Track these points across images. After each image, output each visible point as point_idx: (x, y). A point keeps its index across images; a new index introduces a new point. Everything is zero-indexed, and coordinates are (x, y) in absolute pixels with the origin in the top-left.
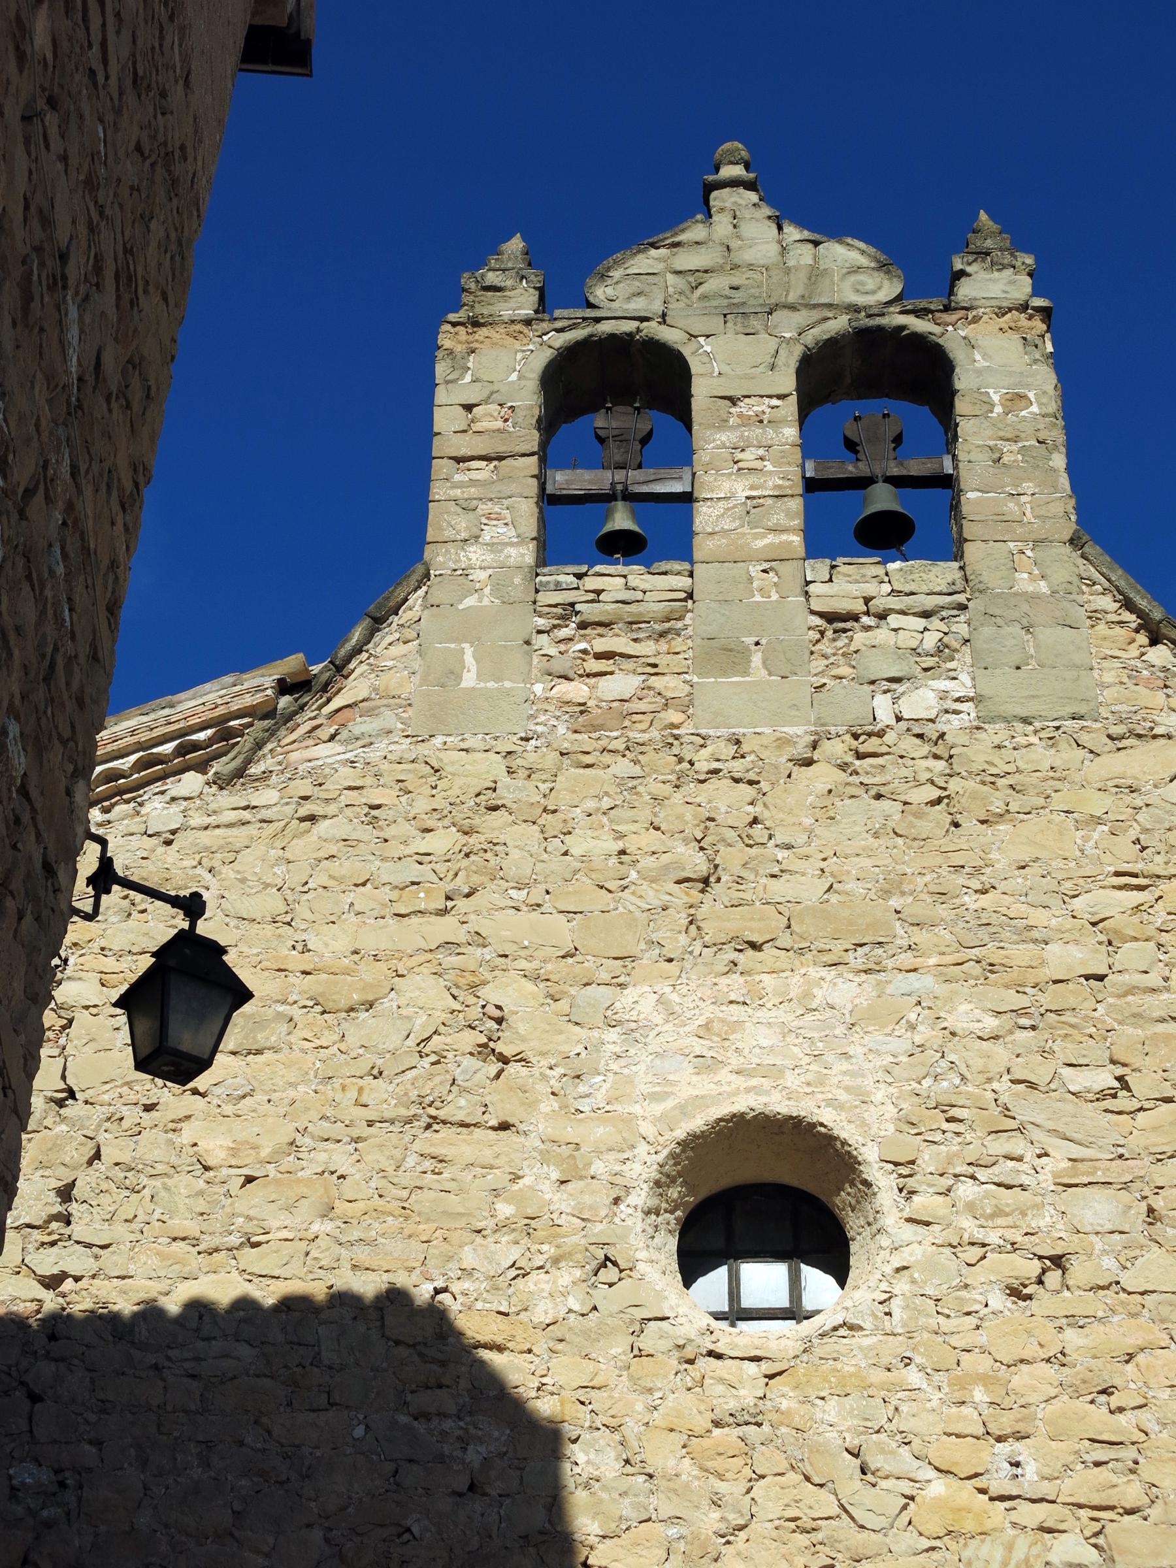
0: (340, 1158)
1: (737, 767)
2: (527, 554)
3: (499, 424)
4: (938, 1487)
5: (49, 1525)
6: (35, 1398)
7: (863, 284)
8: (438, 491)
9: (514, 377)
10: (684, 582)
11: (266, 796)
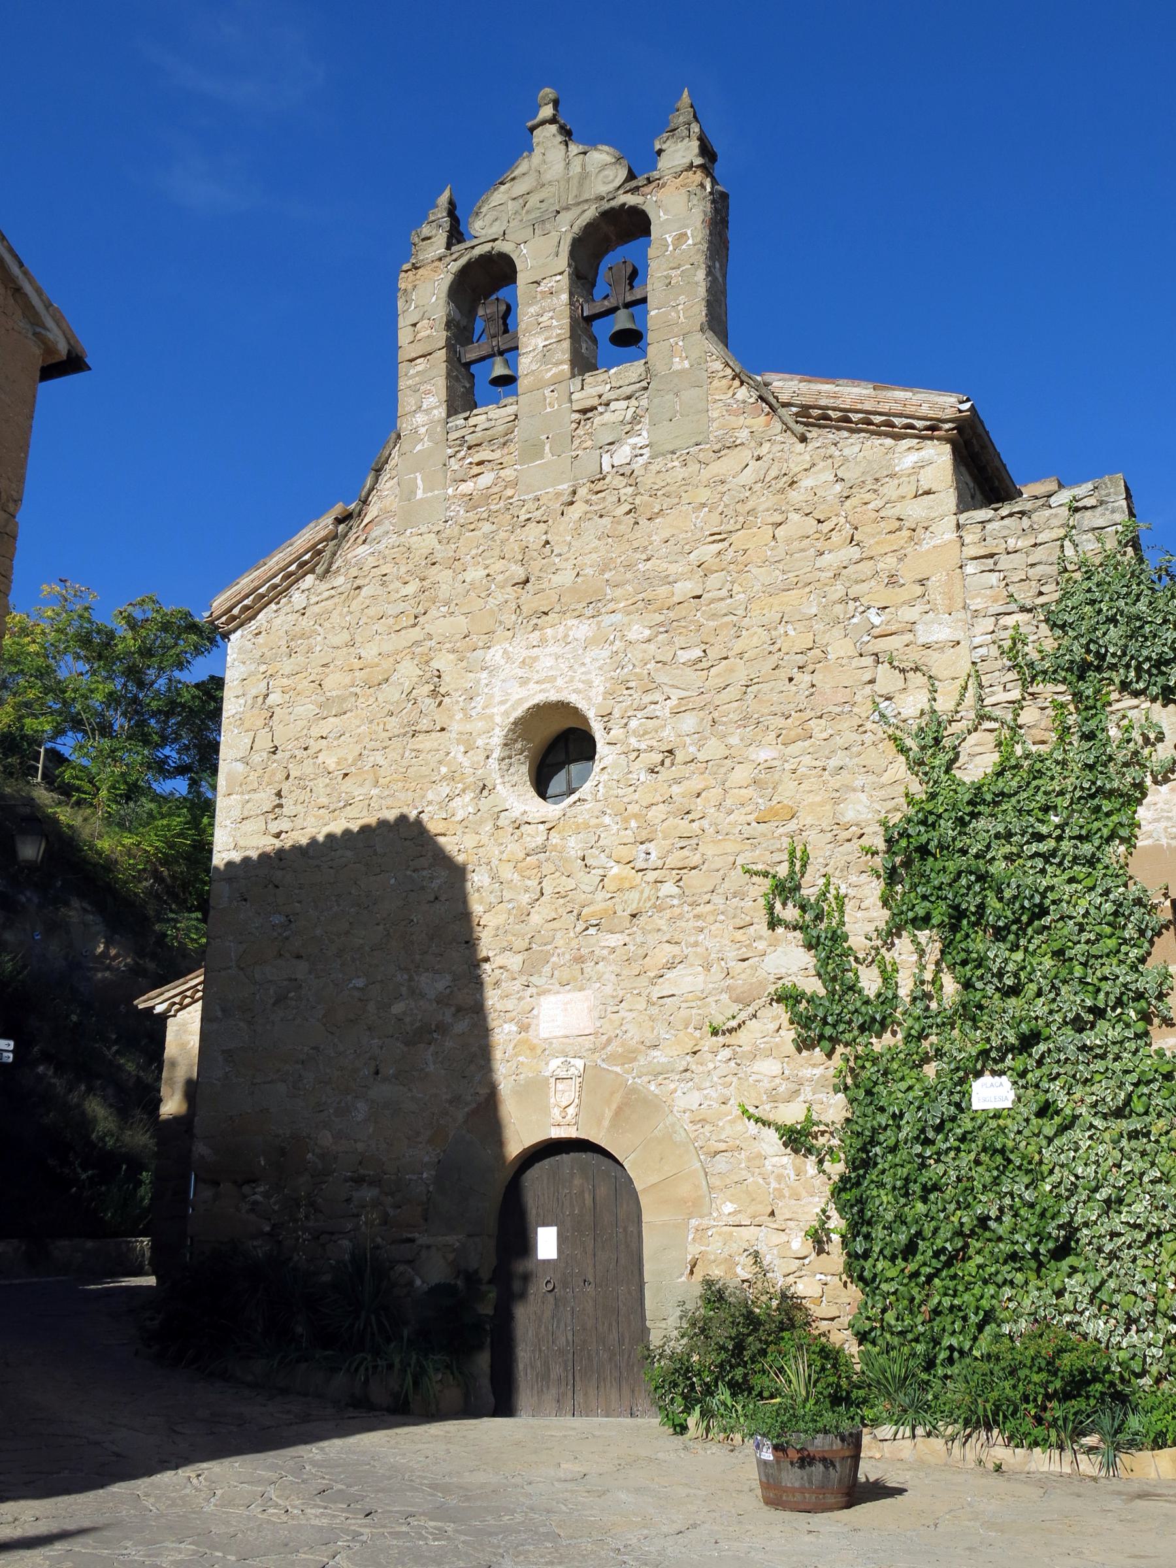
0: (378, 757)
1: (537, 515)
2: (441, 412)
3: (429, 332)
4: (616, 870)
5: (287, 938)
6: (277, 887)
7: (606, 177)
8: (403, 383)
9: (434, 299)
10: (511, 409)
11: (339, 580)
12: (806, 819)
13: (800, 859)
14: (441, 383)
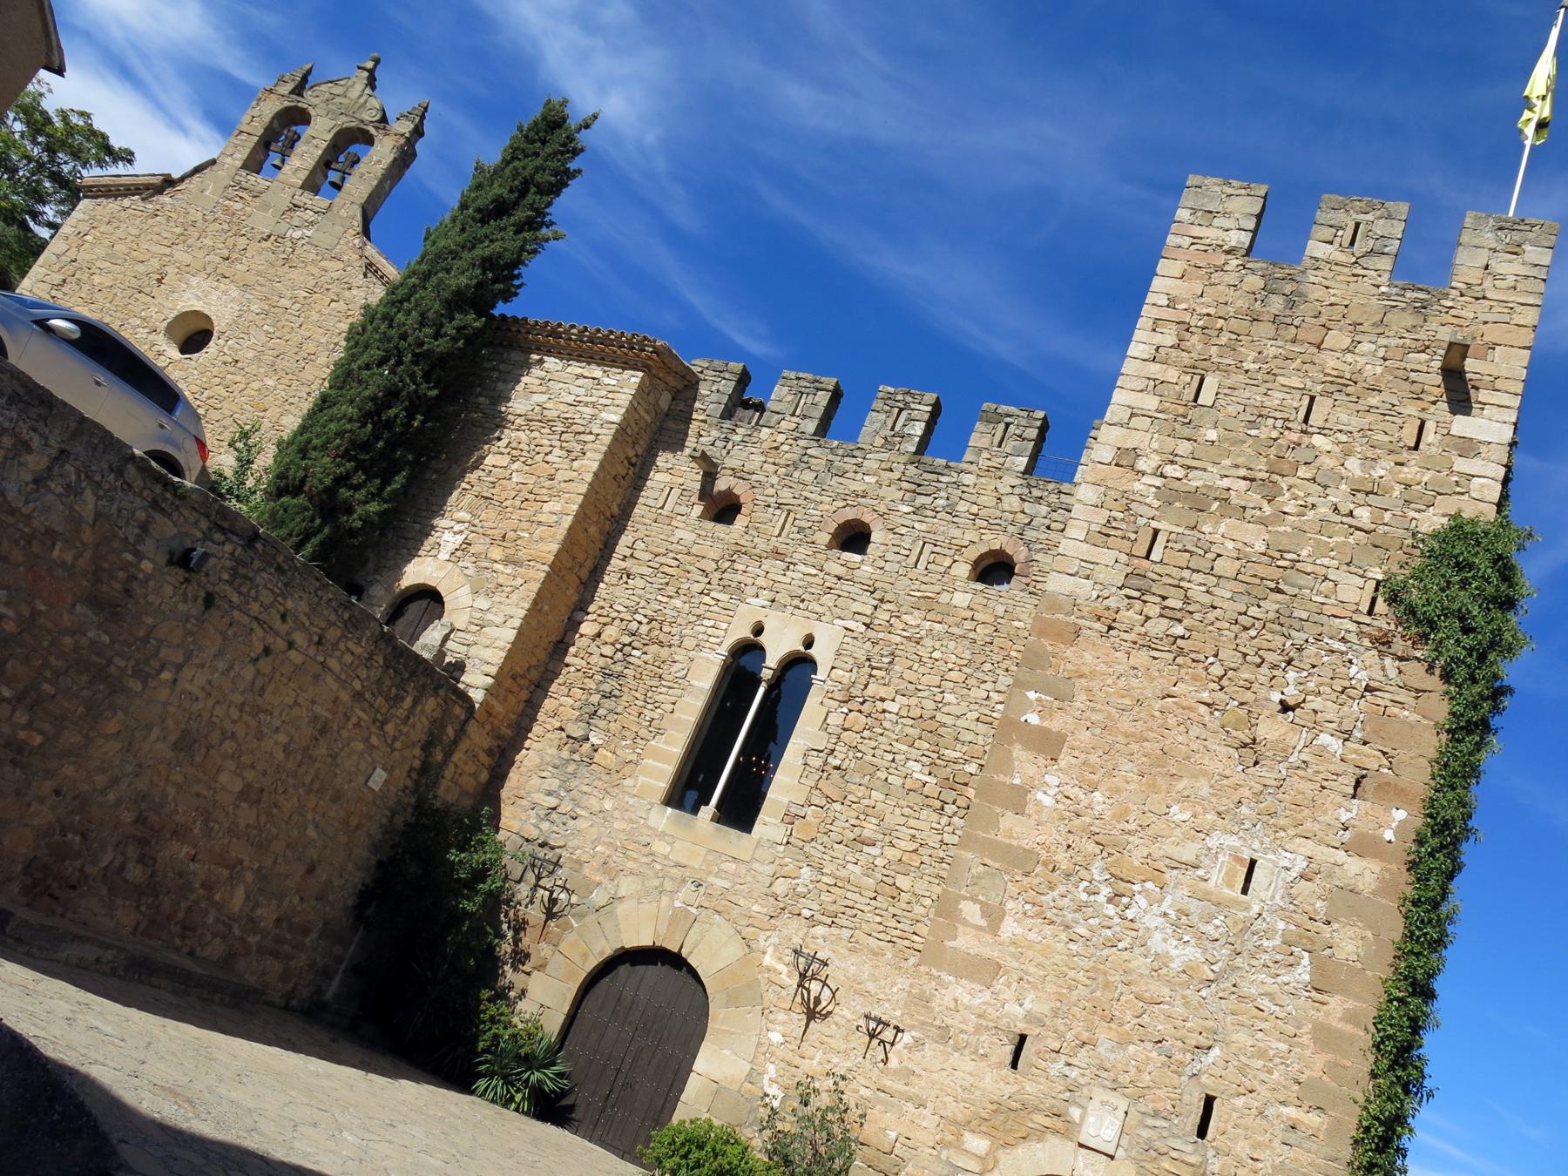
2: (239, 164)
12: (267, 414)
13: (256, 429)
14: (248, 151)
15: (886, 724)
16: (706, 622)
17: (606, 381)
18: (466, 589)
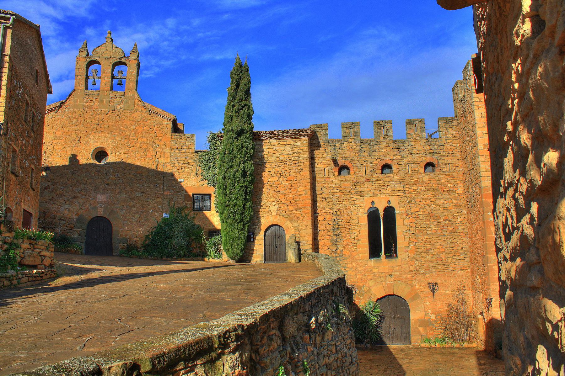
15: (421, 218)
16: (356, 206)
17: (296, 144)
18: (288, 222)
